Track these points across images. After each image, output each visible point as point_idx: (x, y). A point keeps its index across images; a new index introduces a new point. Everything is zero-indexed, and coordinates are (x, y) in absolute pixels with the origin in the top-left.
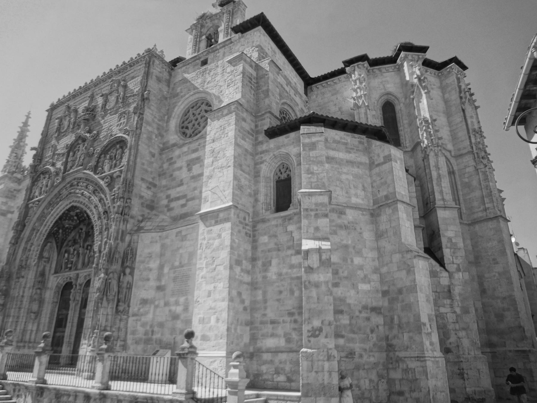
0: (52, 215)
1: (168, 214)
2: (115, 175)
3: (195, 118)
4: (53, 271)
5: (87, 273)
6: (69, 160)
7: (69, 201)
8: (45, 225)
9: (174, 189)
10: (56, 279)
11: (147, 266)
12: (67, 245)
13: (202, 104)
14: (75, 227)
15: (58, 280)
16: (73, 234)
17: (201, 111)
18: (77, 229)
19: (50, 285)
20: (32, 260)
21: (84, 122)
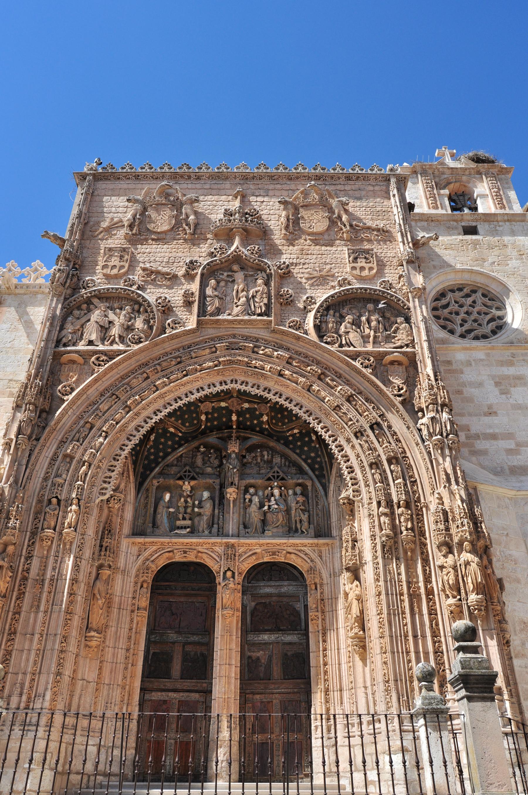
0: (161, 396)
1: (474, 459)
2: (388, 358)
3: (465, 309)
4: (126, 530)
5: (265, 547)
6: (209, 291)
7: (220, 378)
8: (137, 414)
9: (475, 419)
10: (135, 550)
11: (508, 552)
12: (161, 473)
13: (474, 292)
14: (186, 439)
15: (146, 554)
16: (181, 451)
17: (474, 302)
18: (195, 444)
19: (121, 563)
20: (95, 490)
21: (242, 234)
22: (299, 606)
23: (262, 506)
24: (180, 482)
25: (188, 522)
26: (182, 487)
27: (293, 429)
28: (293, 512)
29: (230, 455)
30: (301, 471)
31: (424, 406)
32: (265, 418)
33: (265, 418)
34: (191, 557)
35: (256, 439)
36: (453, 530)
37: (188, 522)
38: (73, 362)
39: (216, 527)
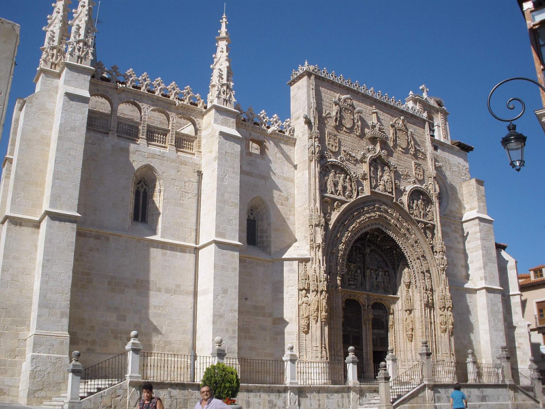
22: (384, 320)
23: (376, 279)
24: (350, 264)
25: (353, 283)
26: (349, 266)
27: (387, 246)
28: (386, 283)
29: (366, 254)
30: (387, 265)
31: (438, 251)
32: (379, 239)
33: (379, 239)
34: (356, 298)
35: (373, 247)
36: (446, 303)
37: (353, 283)
38: (326, 202)
39: (362, 286)
